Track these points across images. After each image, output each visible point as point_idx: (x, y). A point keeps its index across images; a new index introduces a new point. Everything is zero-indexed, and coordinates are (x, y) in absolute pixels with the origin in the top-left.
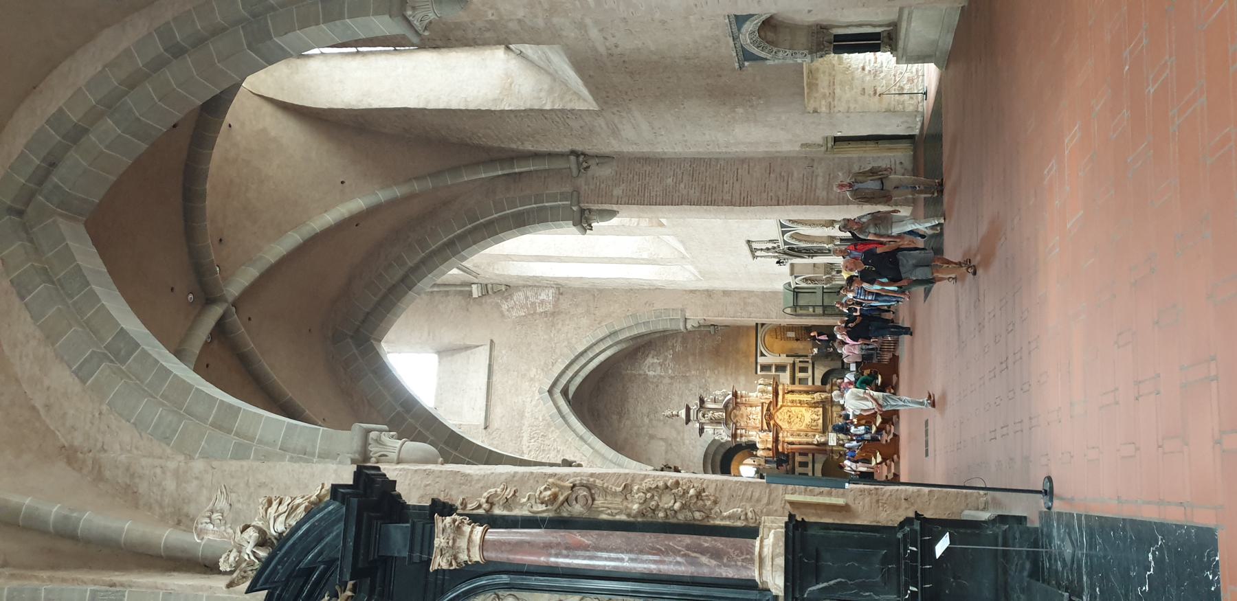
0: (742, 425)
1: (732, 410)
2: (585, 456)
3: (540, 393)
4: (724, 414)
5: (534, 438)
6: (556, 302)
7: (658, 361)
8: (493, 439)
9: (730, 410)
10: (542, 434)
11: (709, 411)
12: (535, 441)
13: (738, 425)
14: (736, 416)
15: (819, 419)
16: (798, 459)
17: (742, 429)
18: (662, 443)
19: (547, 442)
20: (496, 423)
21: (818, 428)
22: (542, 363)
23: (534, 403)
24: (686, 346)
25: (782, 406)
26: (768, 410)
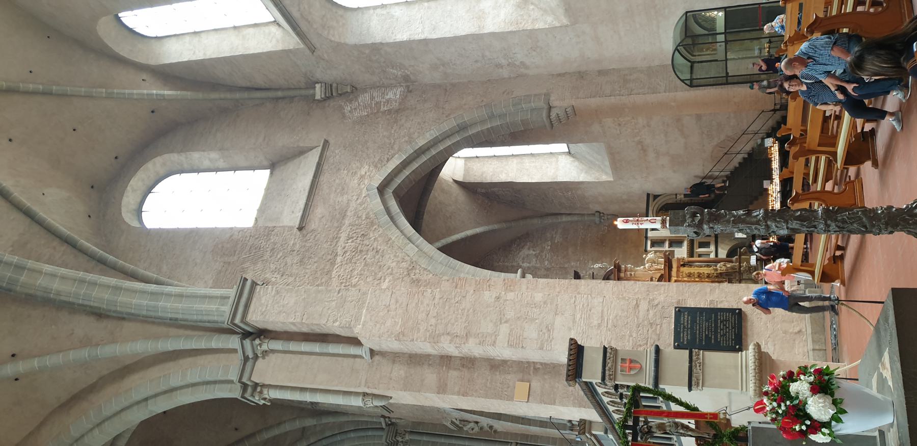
2: (408, 256)
5: (352, 238)
6: (403, 99)
7: (534, 253)
8: (306, 241)
10: (362, 233)
12: (352, 242)
19: (366, 242)
20: (314, 224)
22: (376, 160)
24: (567, 238)
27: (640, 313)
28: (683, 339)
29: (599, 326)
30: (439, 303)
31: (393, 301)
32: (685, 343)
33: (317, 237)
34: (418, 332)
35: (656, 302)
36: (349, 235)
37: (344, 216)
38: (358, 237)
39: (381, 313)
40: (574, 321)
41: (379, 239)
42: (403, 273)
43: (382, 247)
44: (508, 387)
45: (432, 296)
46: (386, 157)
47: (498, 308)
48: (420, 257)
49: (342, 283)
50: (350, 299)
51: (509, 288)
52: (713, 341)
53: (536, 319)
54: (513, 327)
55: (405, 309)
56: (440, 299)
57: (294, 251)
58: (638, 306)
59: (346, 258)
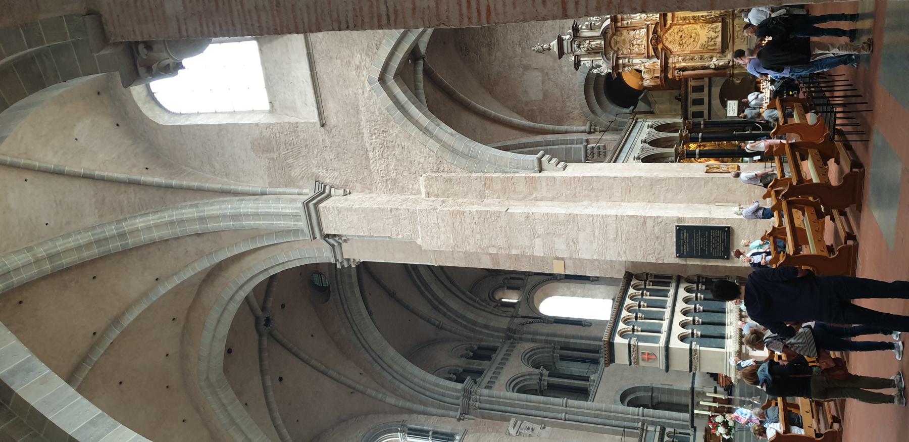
0: (625, 53)
1: (611, 38)
2: (433, 152)
3: (370, 83)
4: (603, 42)
5: (375, 134)
8: (333, 137)
9: (609, 35)
10: (382, 129)
11: (585, 40)
12: (376, 138)
13: (620, 53)
14: (617, 43)
15: (717, 37)
16: (691, 83)
17: (625, 58)
18: (538, 73)
19: (389, 138)
21: (717, 47)
23: (366, 95)
25: (671, 26)
26: (655, 32)
27: (648, 229)
28: (683, 251)
29: (615, 239)
30: (479, 222)
31: (440, 220)
32: (685, 254)
33: (341, 133)
34: (469, 245)
35: (660, 220)
36: (370, 131)
37: (358, 111)
38: (380, 133)
39: (433, 230)
40: (594, 236)
41: (400, 135)
42: (433, 167)
43: (406, 144)
44: (547, 264)
45: (471, 216)
46: (374, 42)
47: (529, 226)
48: (443, 152)
49: (383, 177)
50: (402, 217)
51: (531, 185)
52: (707, 253)
53: (563, 235)
54: (545, 241)
55: (452, 226)
56: (479, 218)
57: (326, 147)
58: (645, 223)
59: (377, 154)
